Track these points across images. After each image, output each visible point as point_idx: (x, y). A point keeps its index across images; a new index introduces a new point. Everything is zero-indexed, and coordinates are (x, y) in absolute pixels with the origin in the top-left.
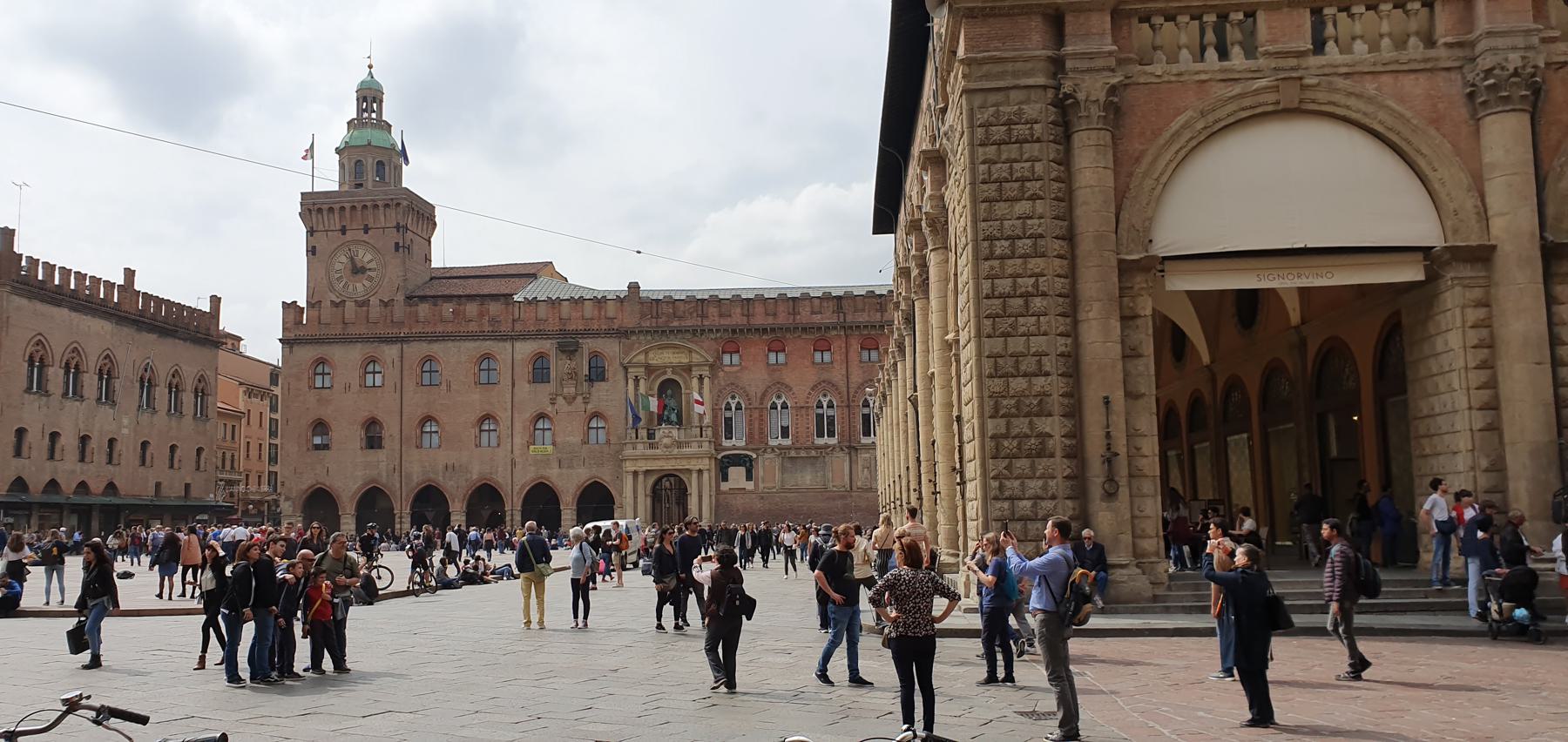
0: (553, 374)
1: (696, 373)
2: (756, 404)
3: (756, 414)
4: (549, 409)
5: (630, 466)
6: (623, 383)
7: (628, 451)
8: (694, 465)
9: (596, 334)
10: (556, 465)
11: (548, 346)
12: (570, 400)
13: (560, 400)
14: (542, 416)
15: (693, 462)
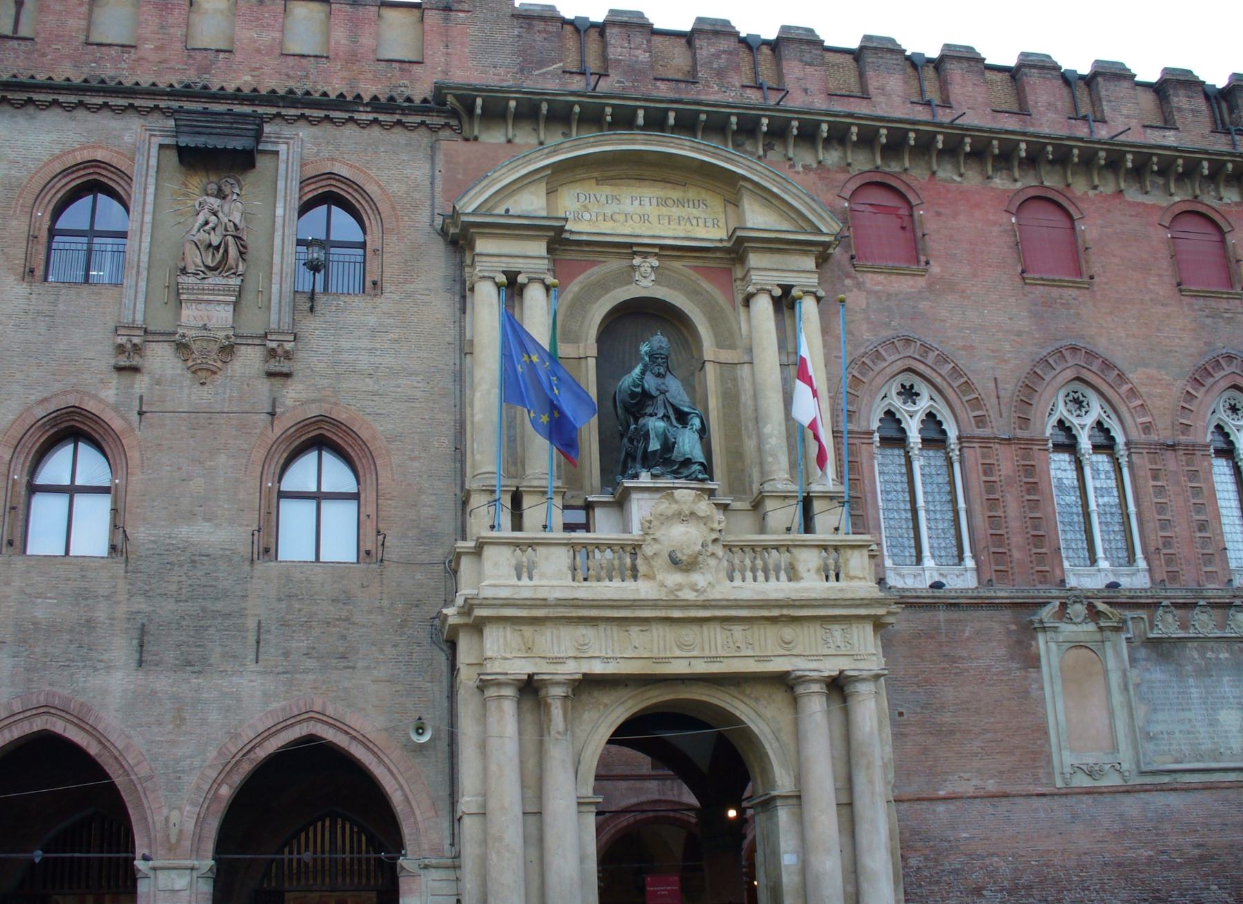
0: (139, 247)
1: (765, 271)
2: (1000, 426)
3: (1006, 461)
4: (106, 397)
5: (506, 655)
6: (441, 306)
7: (494, 577)
8: (813, 654)
9: (335, 109)
10: (121, 649)
11: (133, 141)
12: (205, 357)
13: (160, 358)
14: (71, 428)
15: (807, 638)
